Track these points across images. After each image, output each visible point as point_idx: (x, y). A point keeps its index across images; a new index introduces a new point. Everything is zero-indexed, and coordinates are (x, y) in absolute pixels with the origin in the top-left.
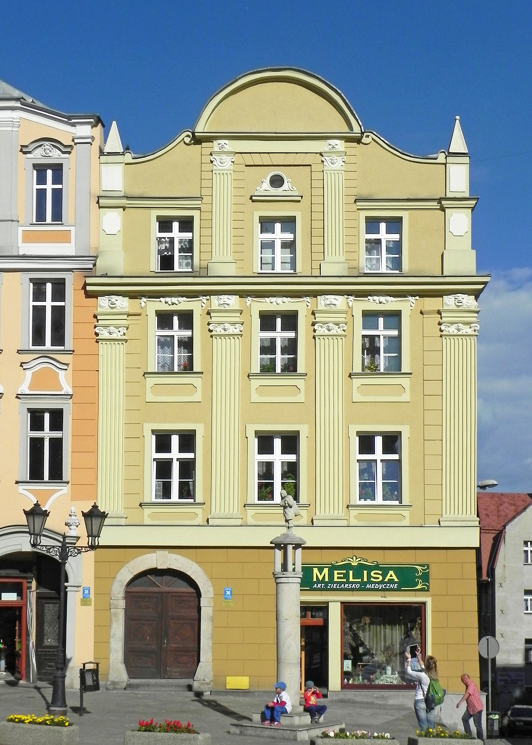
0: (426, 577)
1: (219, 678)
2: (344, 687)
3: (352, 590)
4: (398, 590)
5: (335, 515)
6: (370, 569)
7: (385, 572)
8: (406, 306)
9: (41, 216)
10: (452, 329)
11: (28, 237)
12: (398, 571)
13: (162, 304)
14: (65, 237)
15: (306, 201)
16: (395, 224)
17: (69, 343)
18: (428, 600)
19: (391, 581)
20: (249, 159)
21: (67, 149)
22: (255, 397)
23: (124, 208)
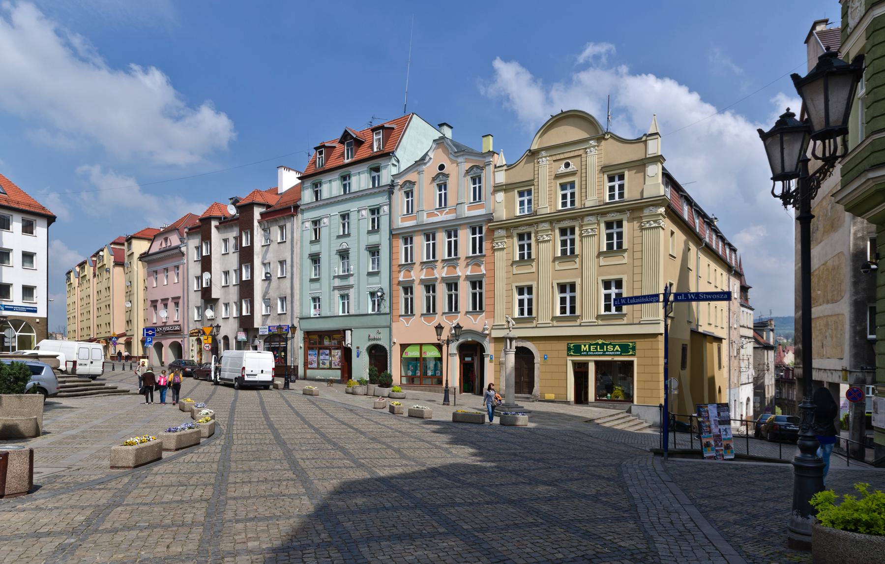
0: (634, 349)
1: (542, 395)
2: (596, 400)
3: (599, 355)
4: (621, 355)
5: (592, 319)
6: (607, 345)
7: (614, 346)
8: (624, 217)
9: (475, 198)
10: (647, 225)
11: (469, 209)
12: (619, 346)
13: (521, 230)
14: (482, 206)
15: (579, 173)
16: (621, 177)
17: (484, 253)
18: (635, 359)
19: (617, 351)
20: (555, 158)
21: (482, 169)
22: (557, 268)
23: (505, 190)
